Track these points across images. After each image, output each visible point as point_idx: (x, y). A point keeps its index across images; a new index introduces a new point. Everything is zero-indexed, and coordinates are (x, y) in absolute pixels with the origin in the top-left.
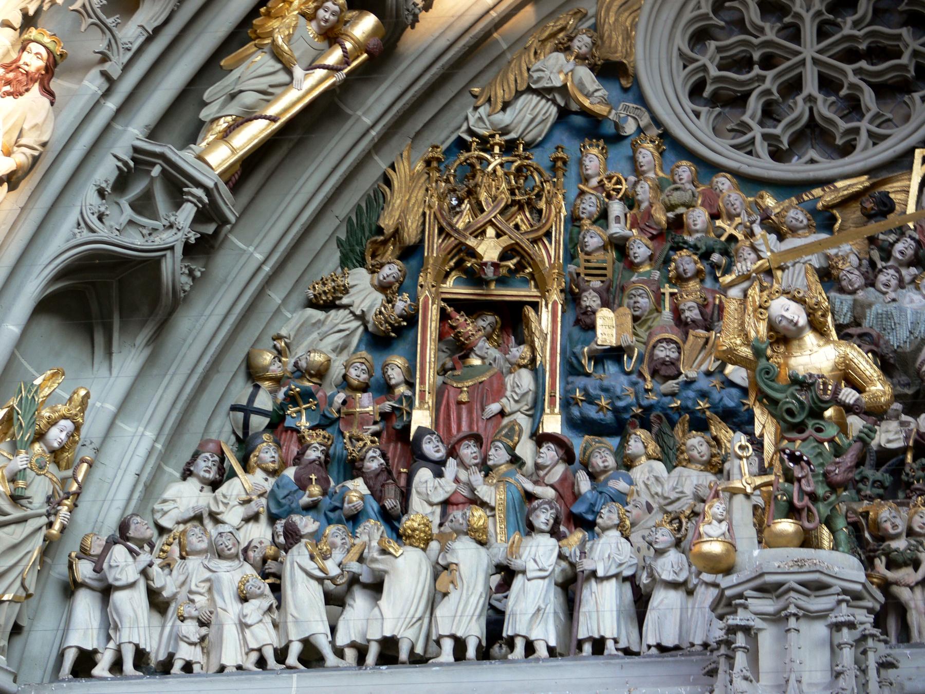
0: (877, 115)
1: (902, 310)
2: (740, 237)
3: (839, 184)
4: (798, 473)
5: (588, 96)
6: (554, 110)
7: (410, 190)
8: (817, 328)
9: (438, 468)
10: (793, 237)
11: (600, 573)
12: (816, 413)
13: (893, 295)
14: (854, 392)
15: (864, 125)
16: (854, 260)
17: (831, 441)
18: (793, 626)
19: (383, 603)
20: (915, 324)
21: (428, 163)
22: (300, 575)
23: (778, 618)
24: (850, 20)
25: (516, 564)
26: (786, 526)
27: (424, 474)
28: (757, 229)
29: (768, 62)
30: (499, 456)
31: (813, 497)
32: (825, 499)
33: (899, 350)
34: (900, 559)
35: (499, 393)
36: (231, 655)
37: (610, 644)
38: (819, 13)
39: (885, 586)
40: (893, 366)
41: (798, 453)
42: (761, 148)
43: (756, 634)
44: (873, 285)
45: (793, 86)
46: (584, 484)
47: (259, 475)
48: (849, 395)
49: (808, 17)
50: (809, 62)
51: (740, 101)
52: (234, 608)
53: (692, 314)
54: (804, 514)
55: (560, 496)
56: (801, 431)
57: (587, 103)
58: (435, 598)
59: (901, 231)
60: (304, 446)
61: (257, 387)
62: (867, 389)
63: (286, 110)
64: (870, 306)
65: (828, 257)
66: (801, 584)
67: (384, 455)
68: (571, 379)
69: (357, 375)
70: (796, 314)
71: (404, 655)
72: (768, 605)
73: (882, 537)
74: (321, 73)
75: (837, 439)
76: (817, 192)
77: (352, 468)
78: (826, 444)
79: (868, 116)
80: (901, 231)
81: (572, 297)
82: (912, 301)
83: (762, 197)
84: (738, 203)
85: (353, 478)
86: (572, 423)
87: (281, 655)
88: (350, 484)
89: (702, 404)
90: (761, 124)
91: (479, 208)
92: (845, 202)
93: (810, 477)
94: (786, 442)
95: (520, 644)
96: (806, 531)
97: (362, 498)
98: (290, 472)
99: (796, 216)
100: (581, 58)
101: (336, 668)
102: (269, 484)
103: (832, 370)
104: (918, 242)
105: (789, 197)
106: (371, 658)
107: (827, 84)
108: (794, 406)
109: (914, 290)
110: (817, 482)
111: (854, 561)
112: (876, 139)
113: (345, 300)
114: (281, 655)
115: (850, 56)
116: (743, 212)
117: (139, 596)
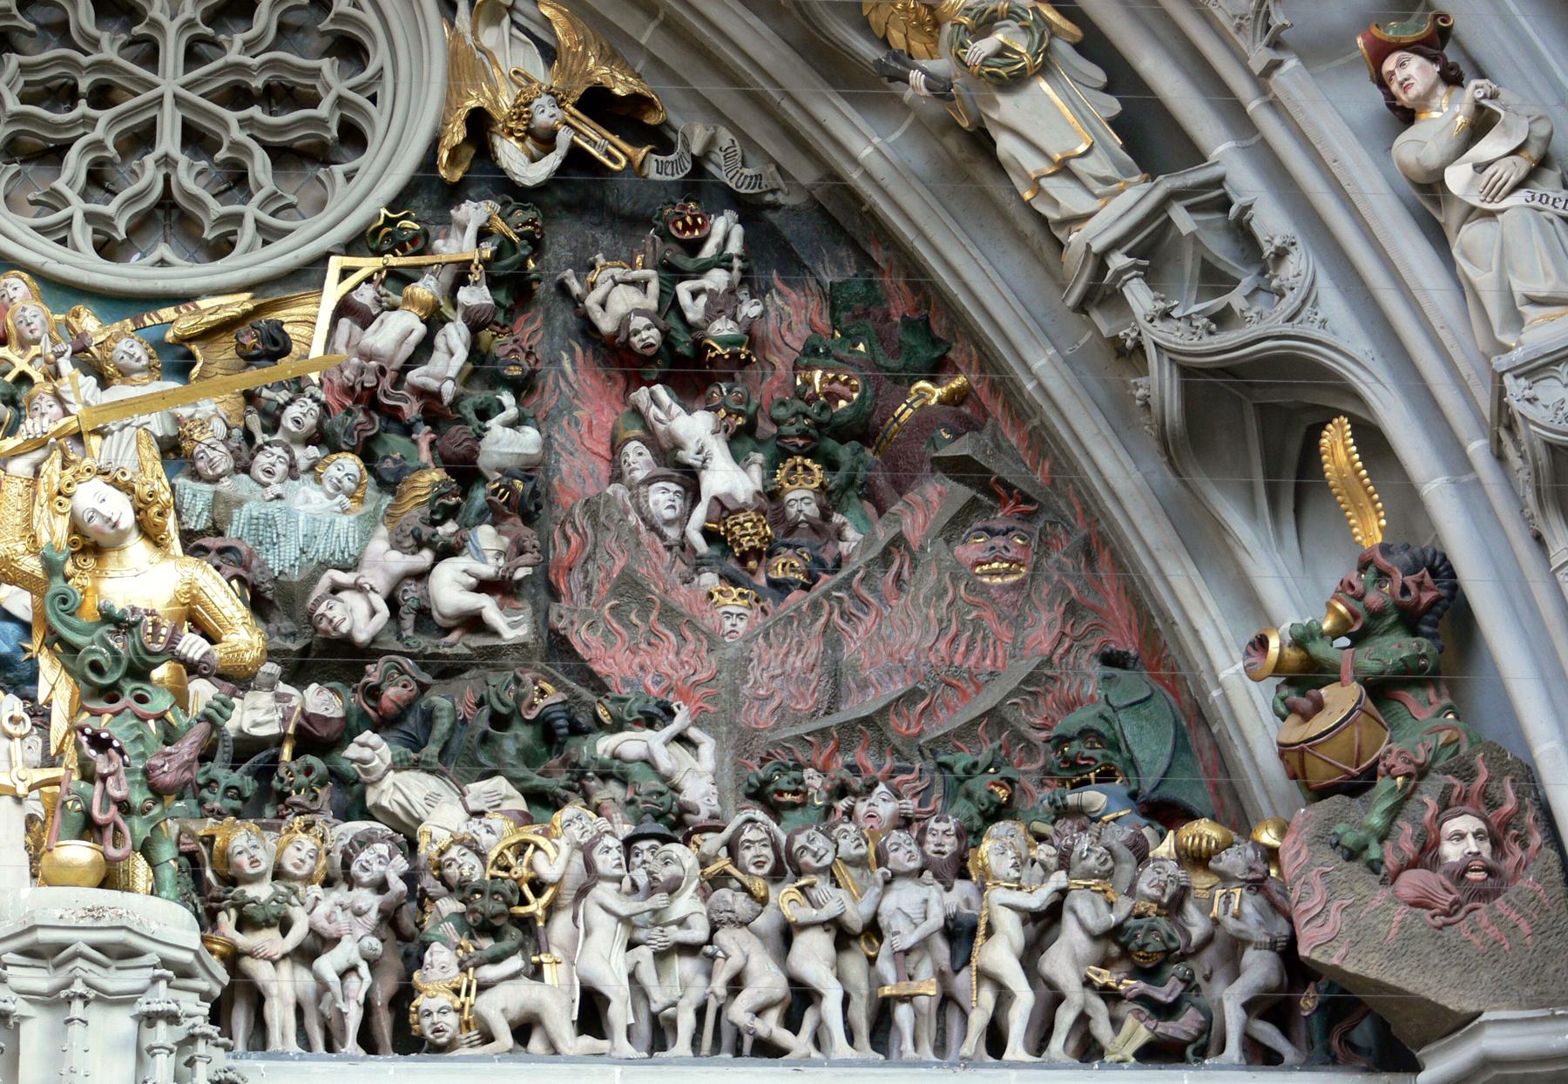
0: (273, 197)
1: (289, 514)
2: (37, 377)
3: (204, 303)
4: (102, 766)
8: (150, 532)
10: (124, 383)
12: (139, 672)
13: (276, 488)
14: (203, 641)
15: (251, 211)
16: (219, 428)
18: (78, 1016)
20: (311, 537)
23: (55, 1001)
24: (239, 38)
26: (79, 853)
28: (65, 365)
29: (102, 96)
31: (125, 807)
32: (144, 811)
33: (281, 578)
34: (260, 916)
38: (190, 24)
39: (233, 959)
40: (271, 602)
41: (104, 735)
42: (82, 234)
43: (17, 1025)
44: (246, 470)
45: (141, 139)
48: (193, 646)
49: (171, 27)
50: (168, 101)
51: (55, 154)
54: (109, 833)
56: (113, 699)
59: (298, 386)
62: (224, 638)
64: (240, 503)
65: (177, 421)
66: (97, 947)
70: (121, 510)
72: (40, 979)
73: (232, 880)
75: (169, 716)
76: (168, 313)
78: (151, 723)
79: (258, 197)
80: (298, 386)
82: (307, 501)
83: (77, 315)
84: (37, 322)
90: (85, 196)
92: (209, 334)
93: (122, 774)
94: (87, 715)
96: (110, 862)
99: (131, 348)
103: (169, 604)
104: (325, 407)
105: (121, 319)
107: (196, 139)
108: (104, 658)
109: (312, 483)
110: (132, 783)
111: (186, 915)
112: (268, 234)
115: (237, 96)
116: (45, 337)
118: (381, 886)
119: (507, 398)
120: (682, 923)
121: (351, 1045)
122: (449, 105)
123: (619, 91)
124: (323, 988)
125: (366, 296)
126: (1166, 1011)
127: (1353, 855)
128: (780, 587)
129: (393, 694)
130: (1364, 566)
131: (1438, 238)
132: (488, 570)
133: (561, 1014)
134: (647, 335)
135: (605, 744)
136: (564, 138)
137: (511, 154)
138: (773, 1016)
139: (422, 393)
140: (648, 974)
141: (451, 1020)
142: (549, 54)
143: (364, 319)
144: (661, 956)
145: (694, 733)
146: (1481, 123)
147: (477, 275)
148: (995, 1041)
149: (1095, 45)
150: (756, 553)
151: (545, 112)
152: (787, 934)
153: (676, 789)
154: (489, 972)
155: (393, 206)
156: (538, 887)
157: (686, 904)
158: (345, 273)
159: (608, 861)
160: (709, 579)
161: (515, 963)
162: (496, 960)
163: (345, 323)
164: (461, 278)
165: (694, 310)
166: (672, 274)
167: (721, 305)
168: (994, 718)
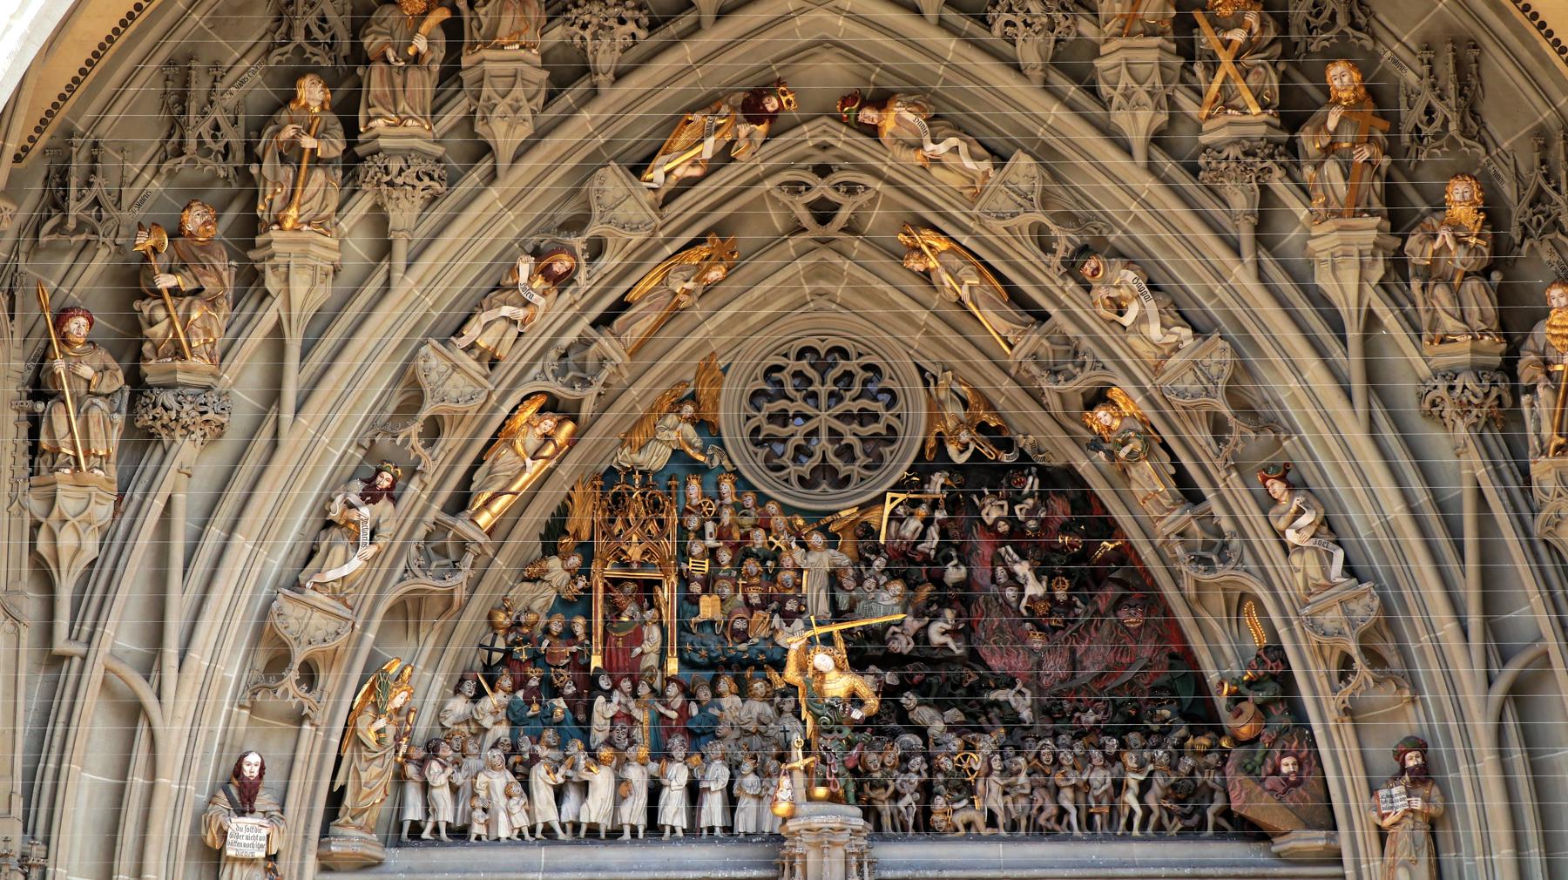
2: (783, 548)
3: (843, 514)
5: (691, 446)
6: (670, 452)
7: (584, 505)
9: (608, 695)
11: (713, 789)
13: (872, 595)
17: (847, 739)
19: (590, 800)
21: (595, 487)
22: (541, 783)
25: (665, 781)
27: (601, 699)
28: (794, 545)
30: (644, 690)
31: (837, 775)
35: (638, 639)
36: (503, 833)
37: (717, 830)
42: (794, 480)
46: (694, 710)
47: (501, 693)
52: (503, 801)
53: (755, 600)
55: (680, 716)
57: (691, 452)
58: (619, 800)
60: (528, 678)
61: (496, 634)
63: (522, 488)
65: (835, 565)
67: (575, 685)
68: (683, 633)
69: (556, 627)
71: (603, 835)
73: (868, 772)
74: (540, 462)
76: (829, 518)
77: (556, 692)
81: (684, 580)
85: (556, 697)
86: (685, 663)
87: (532, 830)
88: (555, 702)
89: (761, 657)
91: (627, 523)
95: (668, 830)
97: (563, 712)
98: (520, 694)
99: (817, 539)
100: (687, 420)
101: (563, 843)
102: (506, 701)
106: (582, 833)
113: (546, 578)
114: (532, 830)
115: (846, 417)
117: (446, 791)
118: (919, 773)
119: (954, 554)
120: (1022, 787)
121: (911, 832)
122: (928, 432)
123: (993, 425)
124: (900, 812)
125: (901, 510)
126: (1188, 816)
127: (1250, 773)
128: (1055, 629)
129: (917, 678)
130: (1258, 656)
131: (1287, 553)
132: (948, 627)
133: (980, 820)
134: (1003, 527)
135: (994, 696)
136: (972, 446)
137: (952, 450)
138: (1053, 820)
139: (922, 553)
140: (1010, 806)
141: (944, 824)
142: (965, 404)
143: (901, 521)
144: (1014, 801)
145: (1024, 690)
146: (1300, 512)
147: (942, 505)
148: (1129, 825)
149: (1165, 445)
150: (1045, 616)
151: (964, 437)
152: (1058, 789)
153: (1018, 713)
154: (956, 806)
155: (909, 471)
156: (972, 771)
157: (1022, 778)
158: (893, 500)
159: (996, 764)
160: (1028, 625)
161: (965, 802)
162: (959, 801)
163: (893, 524)
164: (934, 505)
165: (1021, 517)
166: (1013, 503)
167: (1032, 512)
168: (1131, 683)
